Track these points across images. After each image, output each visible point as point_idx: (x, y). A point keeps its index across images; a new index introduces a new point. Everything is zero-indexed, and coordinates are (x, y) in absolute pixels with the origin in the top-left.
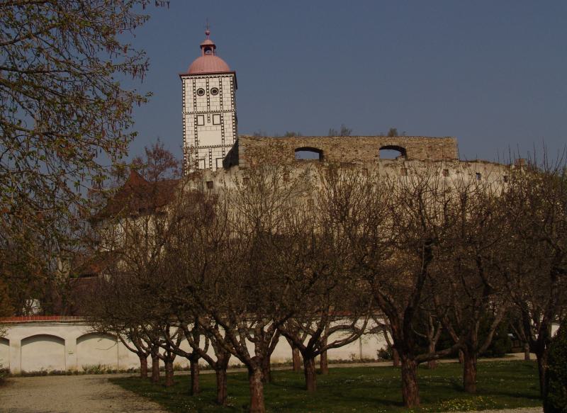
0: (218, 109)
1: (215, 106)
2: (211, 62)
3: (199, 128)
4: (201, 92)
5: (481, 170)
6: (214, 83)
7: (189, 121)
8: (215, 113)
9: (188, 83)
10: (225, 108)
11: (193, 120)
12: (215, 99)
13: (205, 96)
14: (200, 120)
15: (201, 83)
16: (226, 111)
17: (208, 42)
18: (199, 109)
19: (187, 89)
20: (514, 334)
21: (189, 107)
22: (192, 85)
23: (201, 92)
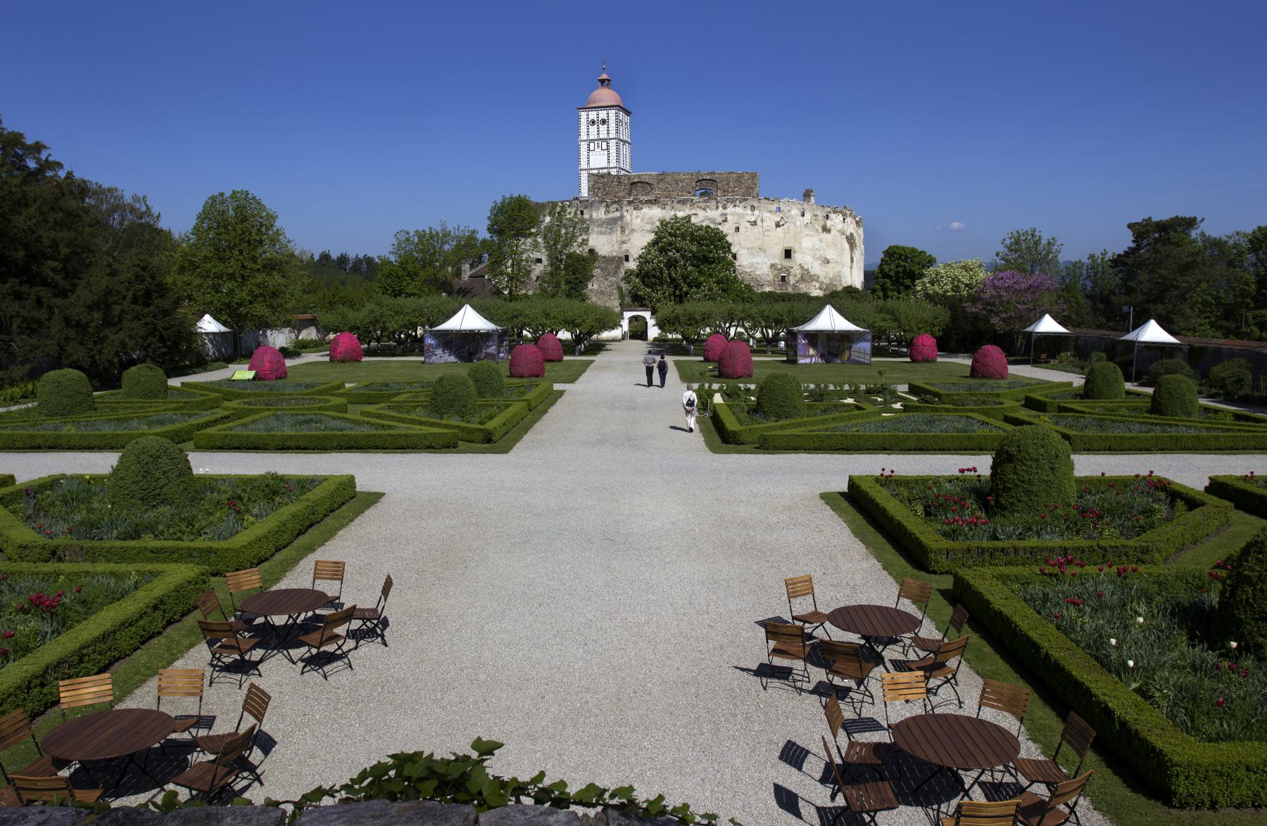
2: (606, 95)
3: (591, 153)
4: (593, 122)
5: (755, 204)
6: (603, 115)
7: (583, 146)
9: (583, 115)
10: (611, 136)
11: (586, 146)
12: (603, 128)
13: (596, 126)
14: (592, 145)
15: (593, 115)
16: (611, 139)
17: (604, 76)
18: (591, 137)
19: (582, 120)
20: (569, 324)
21: (583, 136)
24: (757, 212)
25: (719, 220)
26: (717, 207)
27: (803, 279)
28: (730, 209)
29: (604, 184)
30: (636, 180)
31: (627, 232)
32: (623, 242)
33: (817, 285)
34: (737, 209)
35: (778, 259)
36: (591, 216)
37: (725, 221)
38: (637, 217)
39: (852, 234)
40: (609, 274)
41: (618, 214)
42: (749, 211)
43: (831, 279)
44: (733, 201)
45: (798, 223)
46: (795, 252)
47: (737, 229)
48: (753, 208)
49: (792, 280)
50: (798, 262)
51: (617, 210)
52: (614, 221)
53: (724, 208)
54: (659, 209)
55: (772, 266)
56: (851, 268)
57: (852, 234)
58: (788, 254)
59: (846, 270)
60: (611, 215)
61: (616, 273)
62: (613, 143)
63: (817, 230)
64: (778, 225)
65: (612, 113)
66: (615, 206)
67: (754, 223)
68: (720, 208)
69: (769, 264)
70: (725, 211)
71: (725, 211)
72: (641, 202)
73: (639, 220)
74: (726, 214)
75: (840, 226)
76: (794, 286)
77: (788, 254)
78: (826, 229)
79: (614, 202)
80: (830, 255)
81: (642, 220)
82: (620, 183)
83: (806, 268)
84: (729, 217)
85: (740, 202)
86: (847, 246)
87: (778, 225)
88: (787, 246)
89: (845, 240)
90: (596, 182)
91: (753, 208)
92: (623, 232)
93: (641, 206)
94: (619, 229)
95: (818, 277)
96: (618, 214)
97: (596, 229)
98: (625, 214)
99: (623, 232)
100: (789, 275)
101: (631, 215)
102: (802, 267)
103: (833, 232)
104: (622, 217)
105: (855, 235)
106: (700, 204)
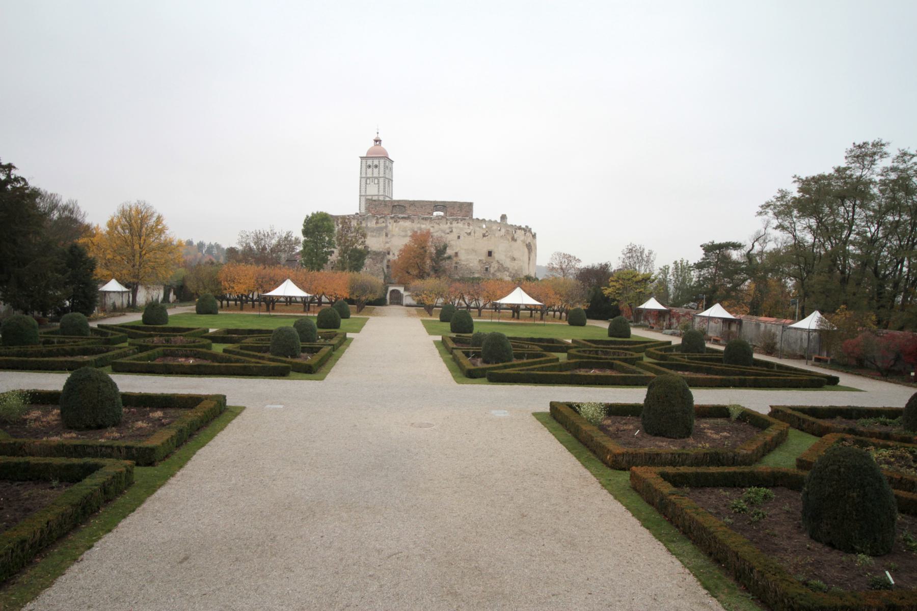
0: (377, 176)
1: (376, 175)
4: (370, 166)
5: (471, 223)
6: (376, 162)
8: (375, 178)
10: (381, 175)
12: (376, 170)
15: (370, 162)
18: (368, 176)
22: (365, 163)
23: (370, 166)
24: (471, 227)
25: (448, 231)
26: (447, 223)
27: (499, 270)
28: (455, 224)
29: (376, 206)
30: (396, 204)
31: (389, 236)
32: (387, 243)
33: (508, 274)
34: (459, 224)
35: (484, 257)
36: (367, 225)
37: (451, 232)
38: (396, 227)
39: (529, 243)
40: (377, 263)
41: (384, 225)
42: (467, 227)
43: (516, 270)
44: (457, 220)
45: (497, 235)
46: (494, 253)
47: (459, 237)
48: (469, 225)
49: (492, 270)
50: (496, 259)
51: (383, 222)
52: (381, 229)
53: (451, 223)
54: (410, 223)
55: (480, 261)
56: (529, 264)
57: (529, 243)
58: (490, 254)
59: (526, 265)
60: (379, 225)
61: (382, 262)
62: (381, 180)
63: (508, 240)
64: (484, 236)
65: (382, 161)
66: (382, 220)
67: (469, 234)
68: (449, 224)
69: (478, 259)
70: (451, 226)
71: (451, 226)
72: (399, 218)
73: (397, 229)
74: (452, 228)
75: (522, 238)
76: (493, 274)
77: (490, 254)
78: (514, 239)
79: (381, 218)
80: (516, 254)
81: (399, 229)
82: (386, 205)
83: (501, 262)
84: (454, 230)
85: (461, 220)
86: (526, 250)
87: (484, 236)
88: (490, 249)
89: (525, 247)
90: (371, 204)
91: (469, 225)
92: (387, 235)
93: (398, 220)
94: (384, 234)
95: (509, 269)
96: (384, 225)
97: (370, 234)
98: (389, 225)
99: (387, 235)
100: (490, 267)
101: (392, 226)
102: (498, 262)
103: (519, 241)
104: (386, 227)
105: (531, 243)
106: (436, 221)
